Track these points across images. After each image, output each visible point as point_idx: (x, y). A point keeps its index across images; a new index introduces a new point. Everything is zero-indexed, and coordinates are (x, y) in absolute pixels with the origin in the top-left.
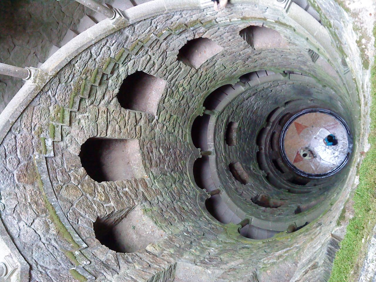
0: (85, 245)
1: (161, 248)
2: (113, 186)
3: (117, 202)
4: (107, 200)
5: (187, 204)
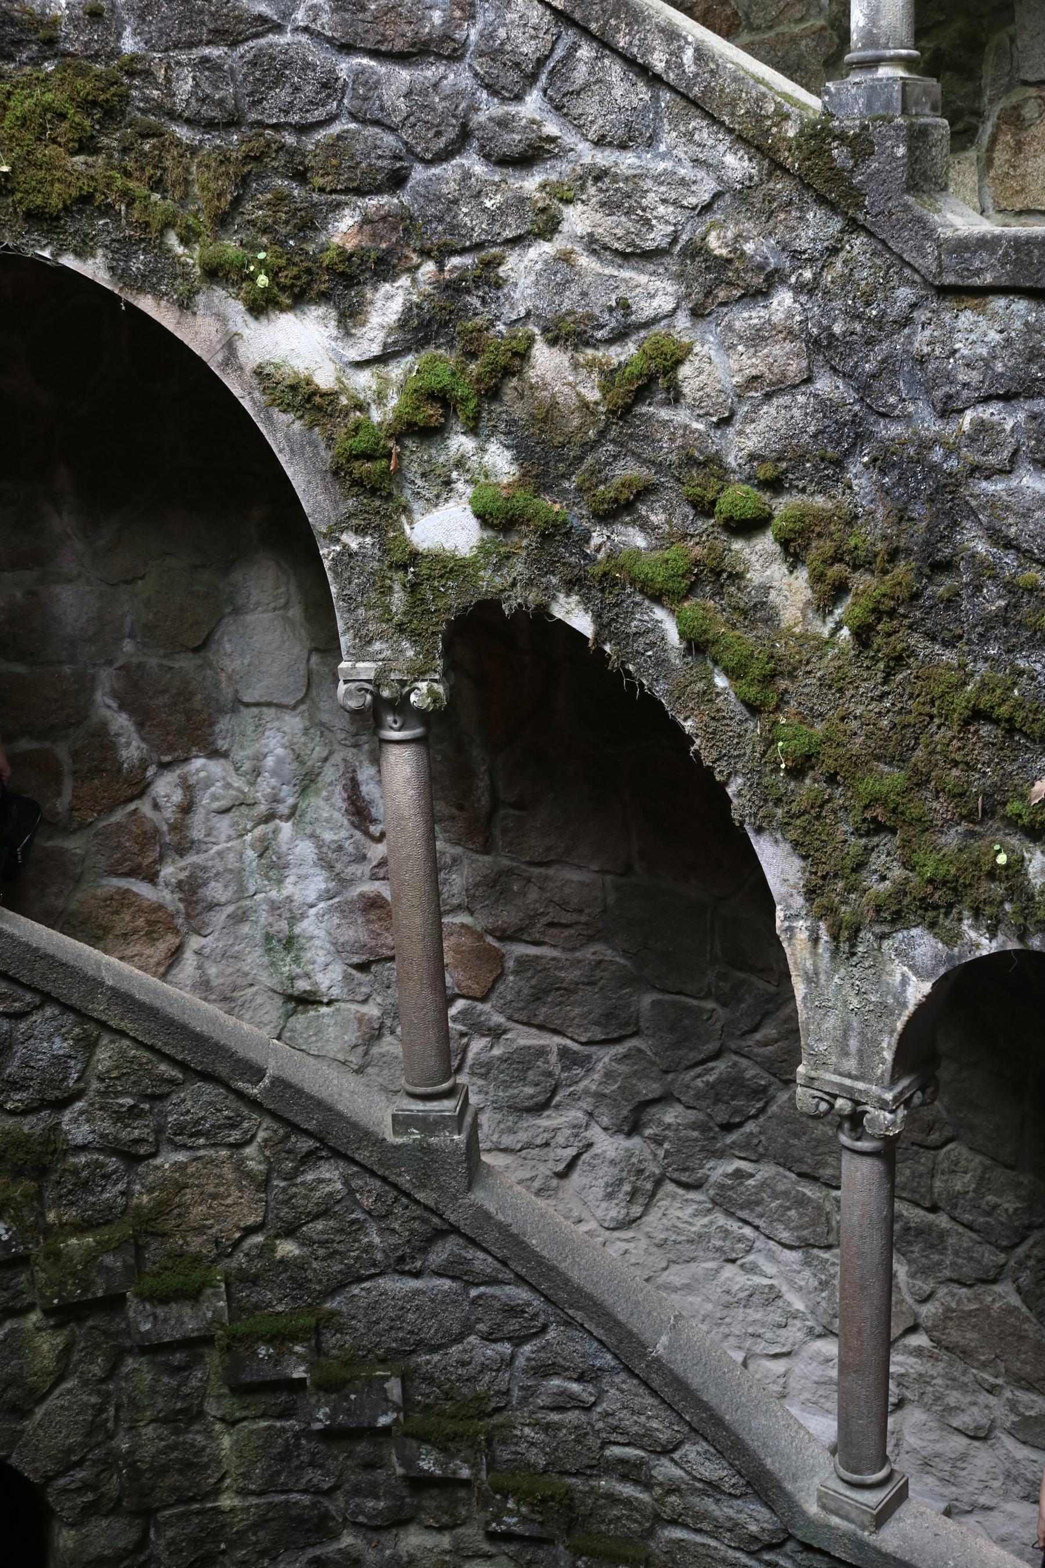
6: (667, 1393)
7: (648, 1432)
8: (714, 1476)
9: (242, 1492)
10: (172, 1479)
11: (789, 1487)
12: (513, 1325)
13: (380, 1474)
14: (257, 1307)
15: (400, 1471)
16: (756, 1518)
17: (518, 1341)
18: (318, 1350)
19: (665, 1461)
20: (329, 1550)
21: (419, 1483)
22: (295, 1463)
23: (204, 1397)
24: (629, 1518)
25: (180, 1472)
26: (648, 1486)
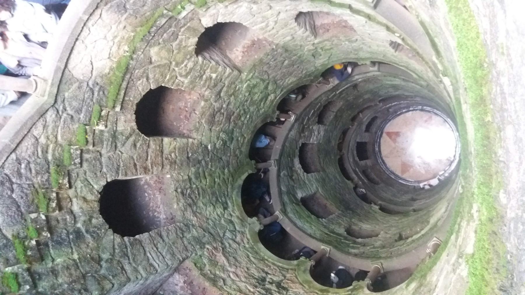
0: (118, 109)
1: (175, 148)
2: (205, 68)
3: (192, 82)
4: (186, 76)
5: (248, 116)
6: (20, 138)
7: (33, 144)
8: (42, 126)
9: (72, 254)
10: (73, 271)
11: (40, 105)
12: (7, 184)
13: (59, 218)
14: (15, 258)
15: (57, 212)
16: (51, 116)
17: (12, 183)
18: (26, 237)
19: (40, 140)
20: (83, 230)
21: (60, 207)
22: (61, 241)
23: (47, 268)
24: (58, 150)
25: (70, 269)
26: (48, 146)
